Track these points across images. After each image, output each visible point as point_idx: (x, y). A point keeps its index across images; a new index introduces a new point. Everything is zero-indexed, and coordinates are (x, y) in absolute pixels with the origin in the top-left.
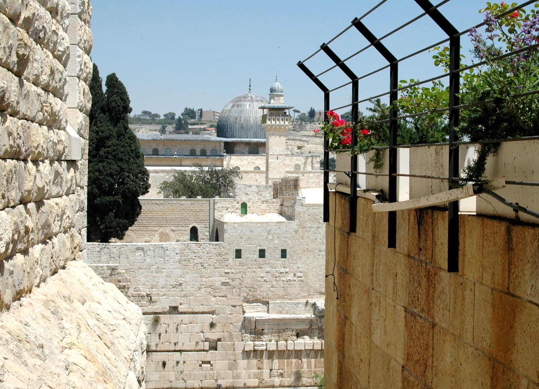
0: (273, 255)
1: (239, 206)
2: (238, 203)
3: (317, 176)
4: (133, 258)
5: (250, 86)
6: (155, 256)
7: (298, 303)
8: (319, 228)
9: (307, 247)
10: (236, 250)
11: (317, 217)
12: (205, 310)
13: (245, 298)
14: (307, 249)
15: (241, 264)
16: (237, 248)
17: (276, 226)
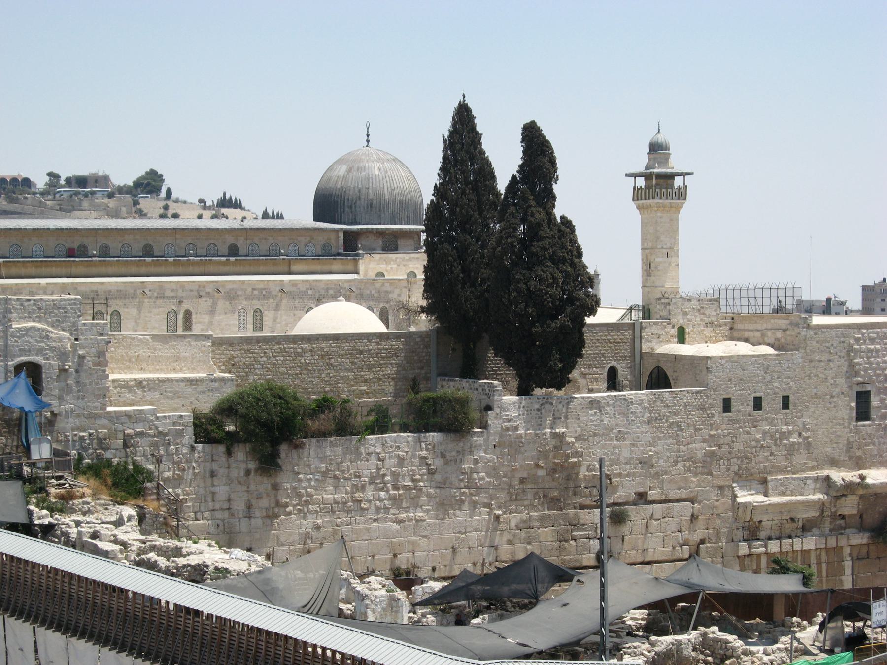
0: (772, 404)
1: (674, 332)
2: (673, 327)
4: (585, 418)
5: (368, 136)
6: (615, 414)
7: (807, 478)
8: (830, 360)
9: (815, 391)
10: (724, 399)
11: (827, 345)
12: (684, 496)
14: (816, 394)
15: (731, 421)
16: (725, 396)
17: (775, 359)
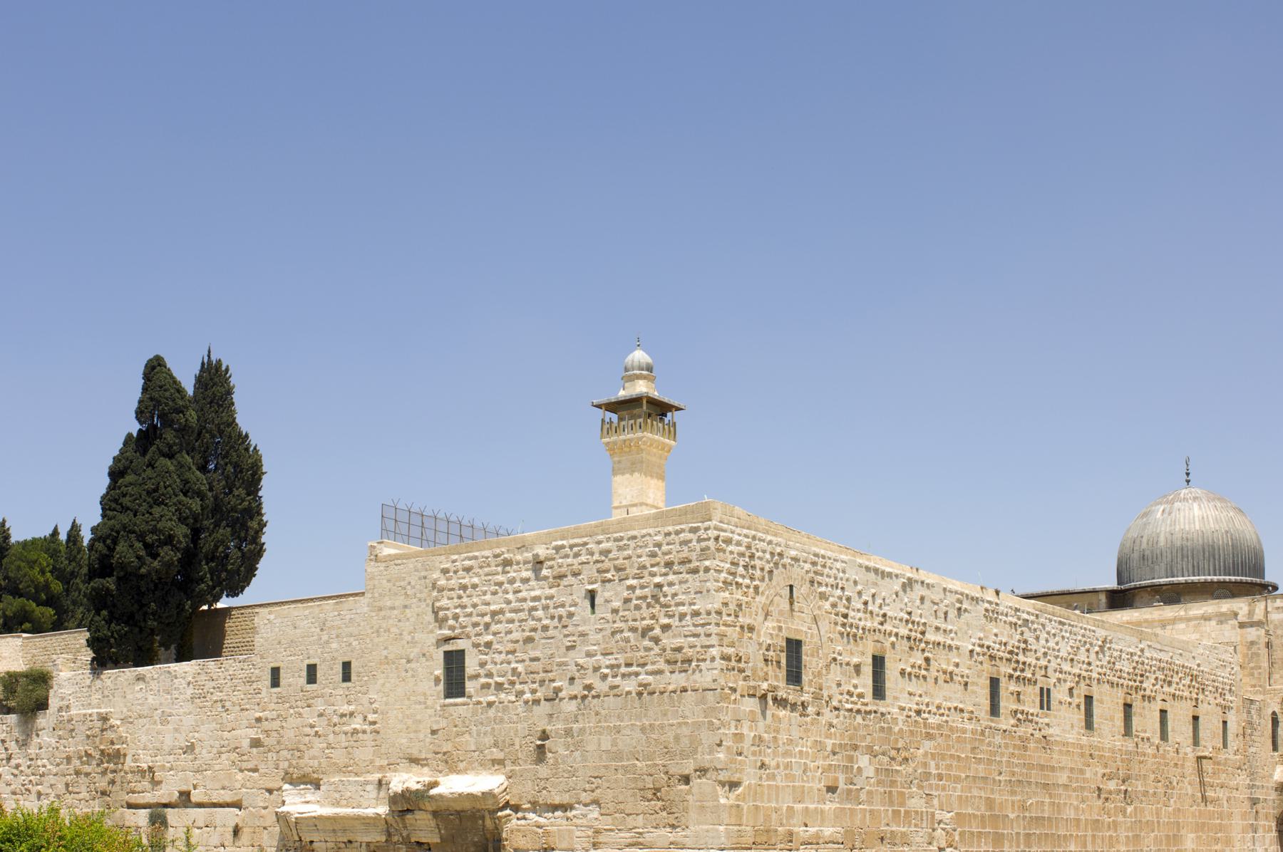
0: (329, 674)
3: (1195, 626)
7: (367, 783)
8: (406, 607)
9: (385, 653)
15: (281, 700)
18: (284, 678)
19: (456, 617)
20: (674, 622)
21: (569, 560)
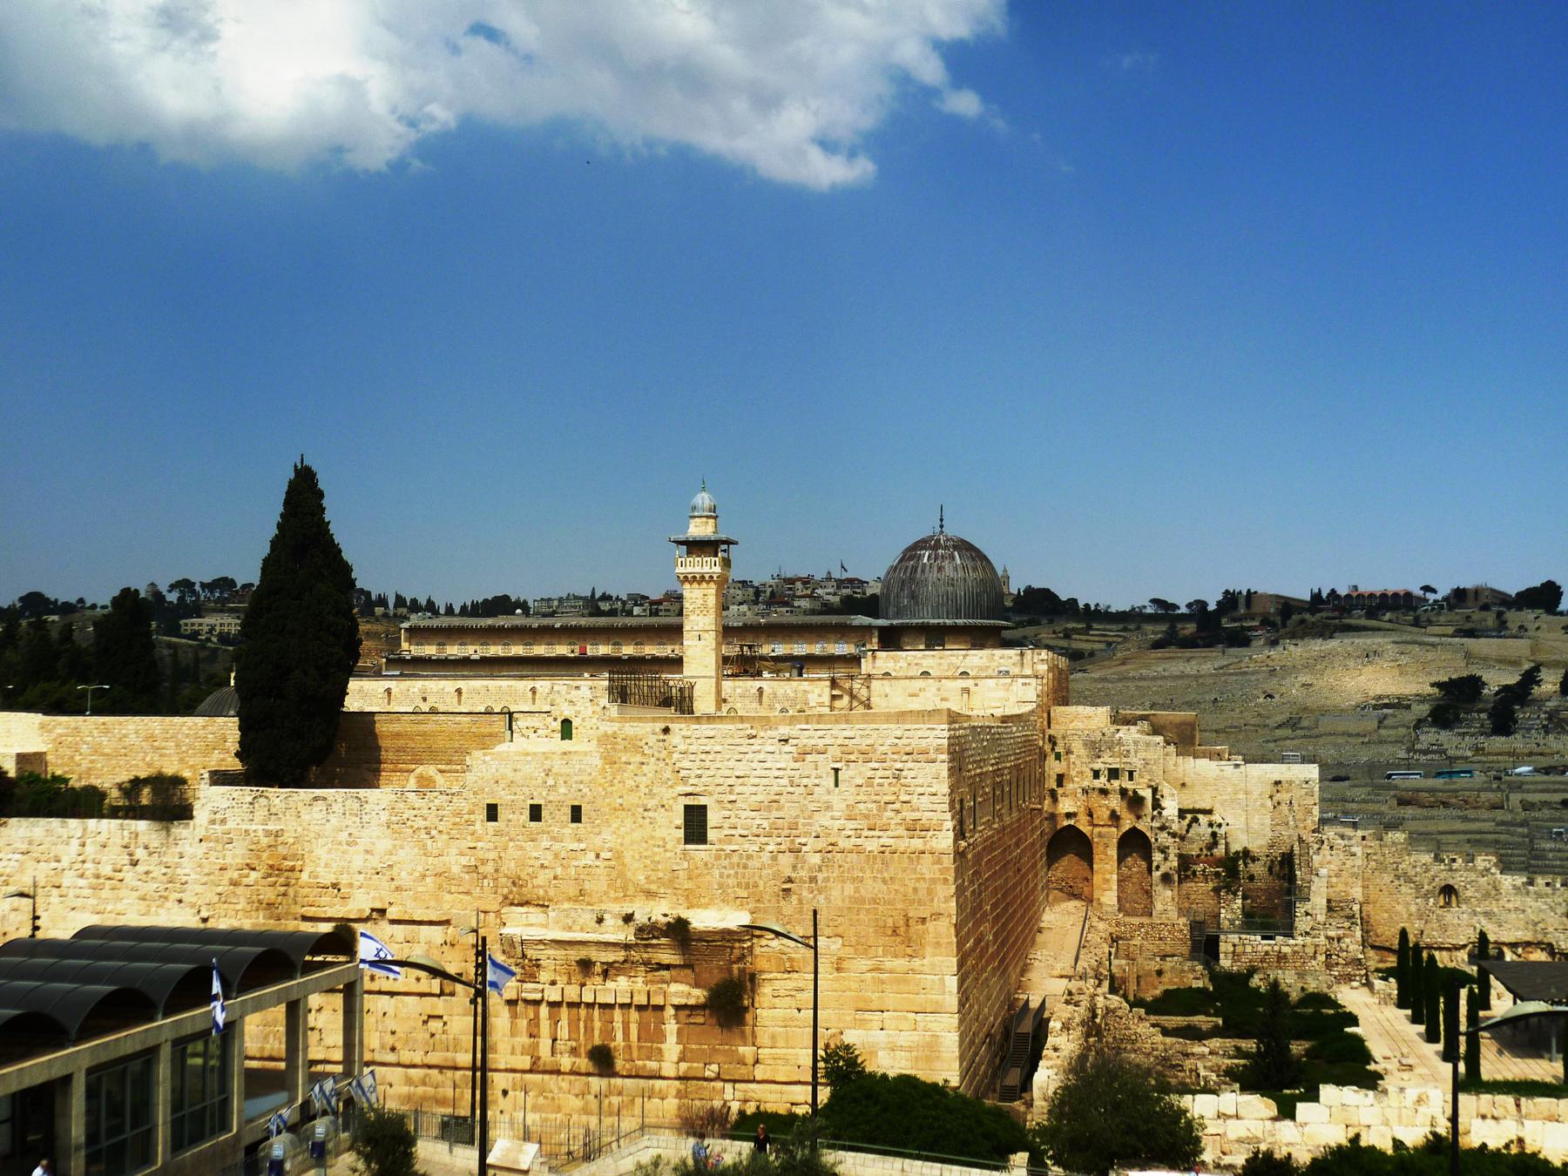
1: (557, 725)
12: (434, 919)
13: (506, 898)
18: (502, 813)
19: (700, 777)
20: (914, 799)
21: (813, 742)
